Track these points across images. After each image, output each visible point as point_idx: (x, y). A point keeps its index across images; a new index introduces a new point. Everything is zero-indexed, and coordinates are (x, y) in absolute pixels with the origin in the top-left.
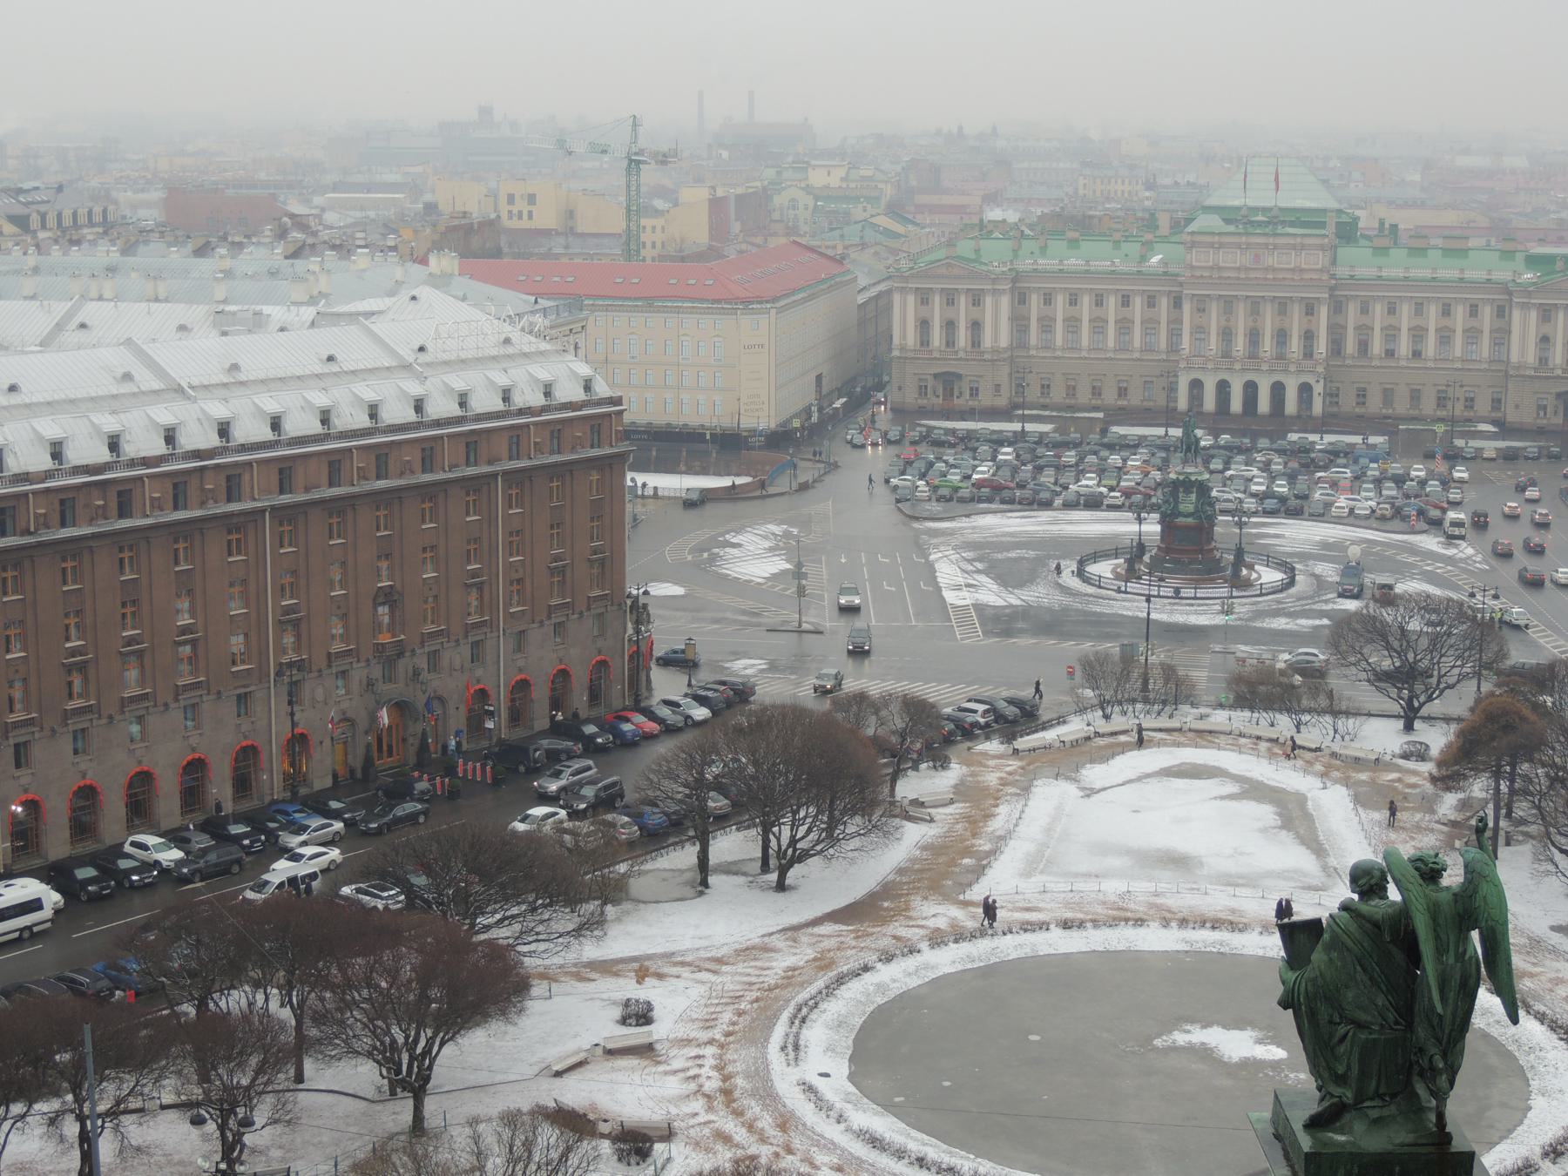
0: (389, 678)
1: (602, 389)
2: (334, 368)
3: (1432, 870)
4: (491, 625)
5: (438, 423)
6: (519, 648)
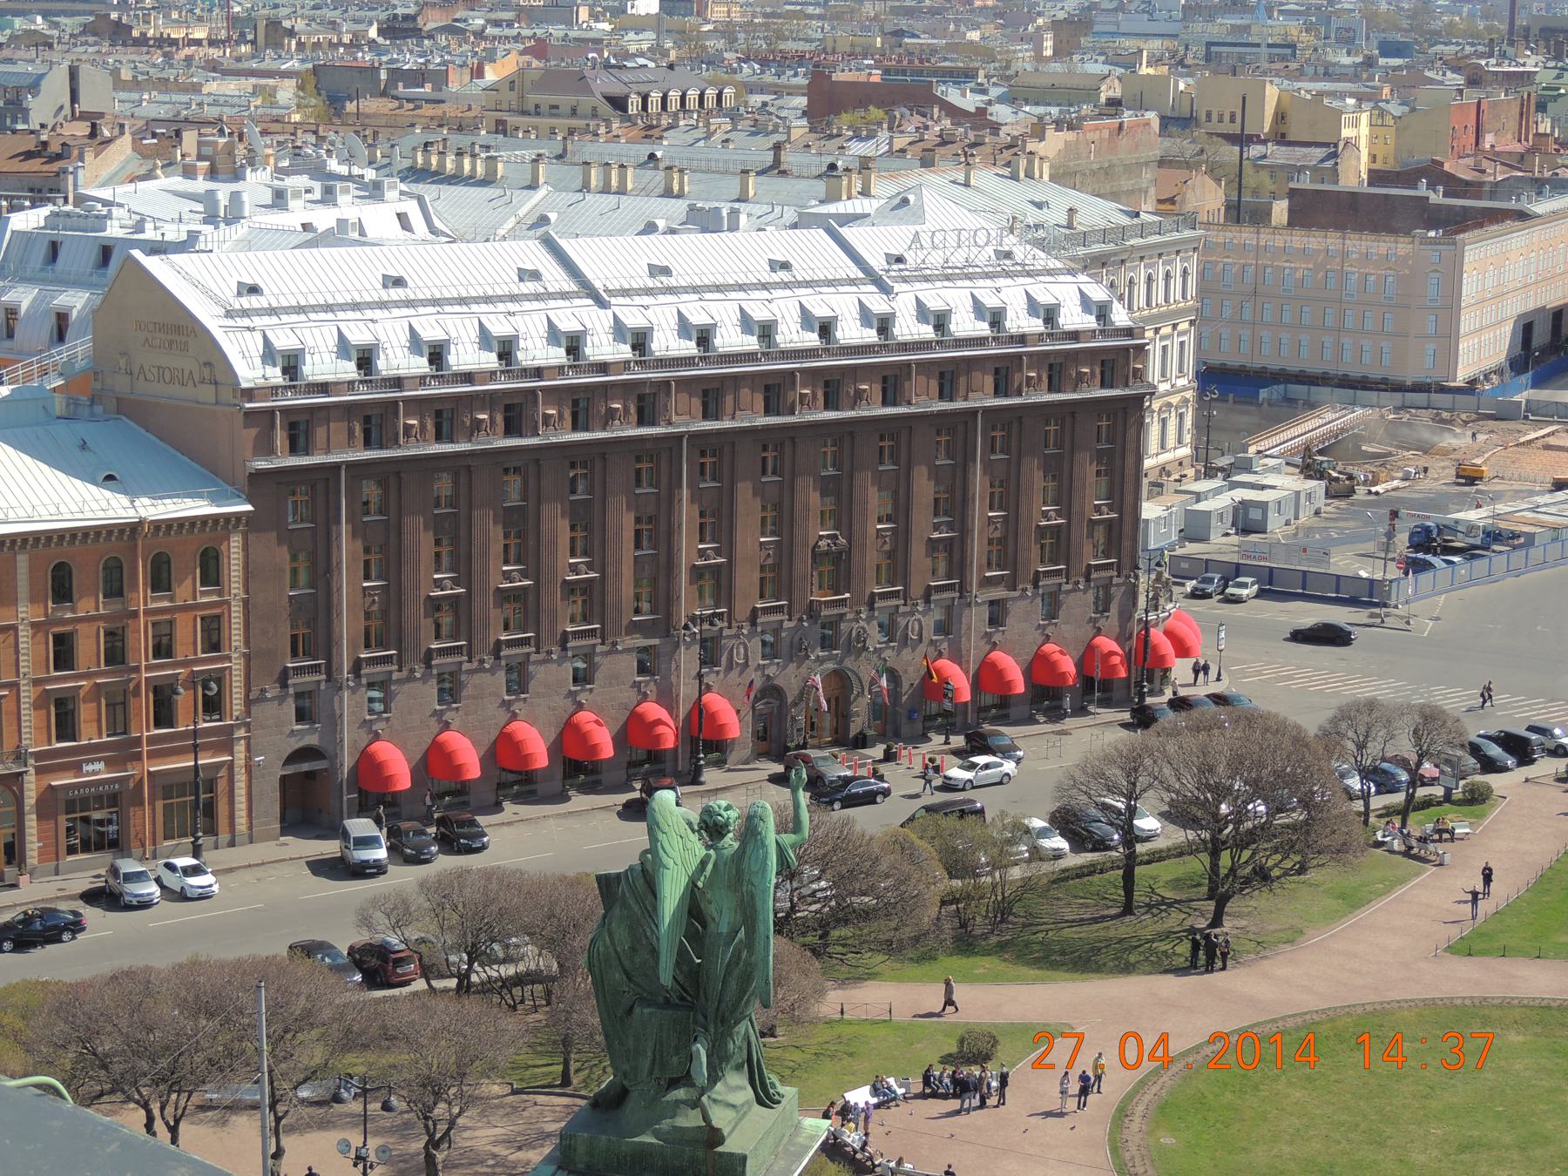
0: (827, 643)
1: (1120, 317)
2: (783, 275)
3: (715, 824)
4: (963, 589)
5: (905, 347)
6: (996, 620)
